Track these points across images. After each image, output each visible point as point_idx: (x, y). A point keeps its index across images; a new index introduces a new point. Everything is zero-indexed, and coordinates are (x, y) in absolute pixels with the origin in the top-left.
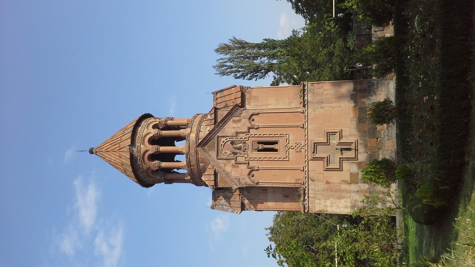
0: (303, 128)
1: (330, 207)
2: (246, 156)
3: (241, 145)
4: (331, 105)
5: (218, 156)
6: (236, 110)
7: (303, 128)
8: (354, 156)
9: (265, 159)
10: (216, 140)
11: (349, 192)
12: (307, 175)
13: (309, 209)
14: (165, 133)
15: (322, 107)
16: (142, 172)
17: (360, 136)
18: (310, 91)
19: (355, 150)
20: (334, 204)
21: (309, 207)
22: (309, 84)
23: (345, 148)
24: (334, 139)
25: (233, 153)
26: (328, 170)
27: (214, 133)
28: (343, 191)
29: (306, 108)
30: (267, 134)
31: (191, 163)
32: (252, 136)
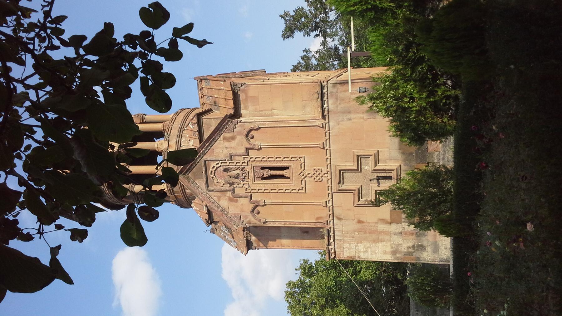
0: (324, 148)
1: (364, 252)
3: (238, 171)
4: (362, 115)
5: (208, 186)
6: (227, 124)
9: (273, 191)
10: (203, 165)
11: (389, 234)
12: (331, 212)
13: (335, 254)
15: (350, 119)
17: (405, 160)
18: (332, 96)
19: (397, 179)
21: (335, 252)
22: (329, 85)
24: (367, 164)
26: (359, 206)
28: (381, 232)
29: (327, 120)
30: (273, 157)
32: (252, 159)
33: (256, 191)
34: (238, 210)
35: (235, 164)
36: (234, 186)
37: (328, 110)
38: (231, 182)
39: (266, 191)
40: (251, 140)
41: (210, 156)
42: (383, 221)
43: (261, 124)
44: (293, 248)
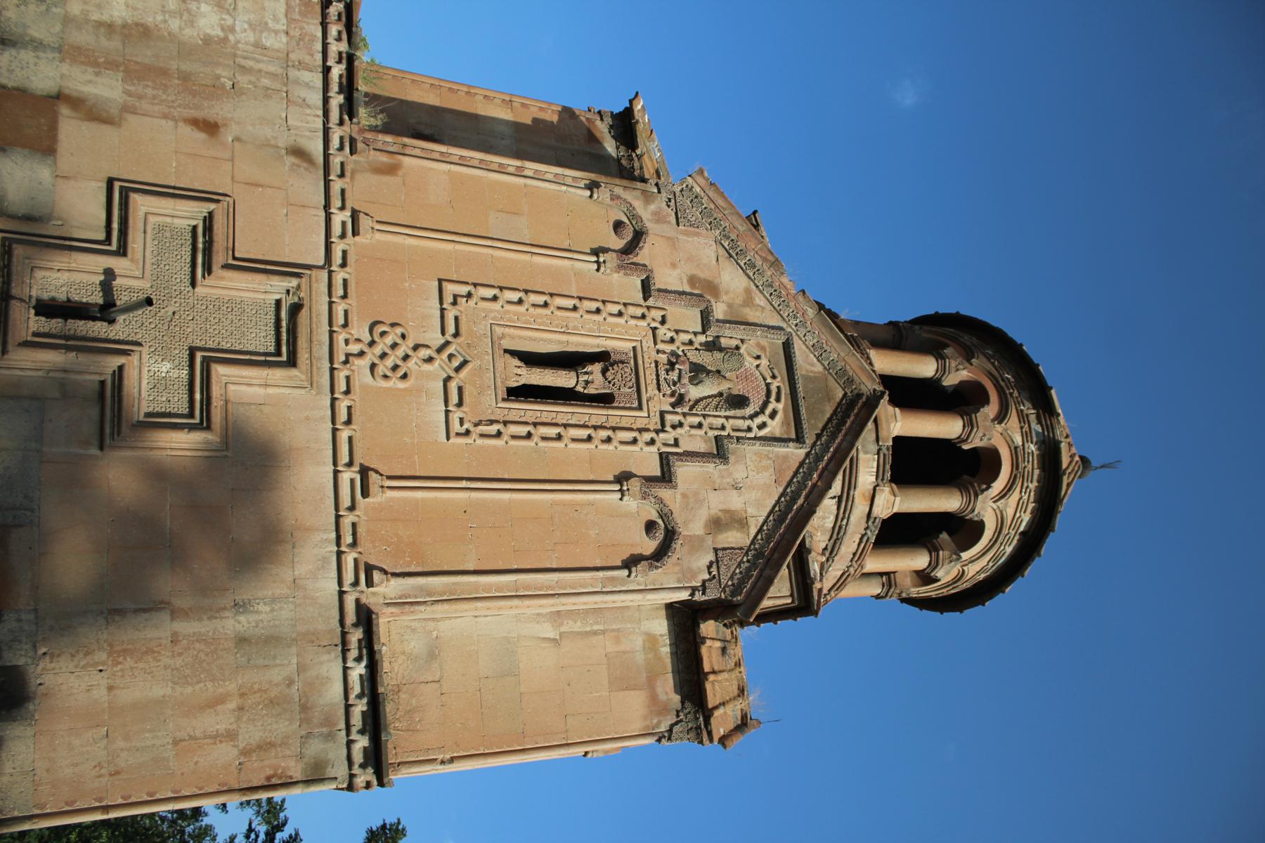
0: (364, 471)
3: (694, 392)
5: (787, 347)
6: (742, 582)
12: (336, 186)
14: (946, 502)
18: (328, 721)
21: (324, 26)
22: (341, 771)
24: (159, 384)
27: (819, 458)
28: (112, 65)
32: (647, 436)
36: (702, 339)
37: (345, 651)
38: (718, 355)
39: (593, 306)
40: (654, 516)
41: (785, 458)
43: (622, 582)
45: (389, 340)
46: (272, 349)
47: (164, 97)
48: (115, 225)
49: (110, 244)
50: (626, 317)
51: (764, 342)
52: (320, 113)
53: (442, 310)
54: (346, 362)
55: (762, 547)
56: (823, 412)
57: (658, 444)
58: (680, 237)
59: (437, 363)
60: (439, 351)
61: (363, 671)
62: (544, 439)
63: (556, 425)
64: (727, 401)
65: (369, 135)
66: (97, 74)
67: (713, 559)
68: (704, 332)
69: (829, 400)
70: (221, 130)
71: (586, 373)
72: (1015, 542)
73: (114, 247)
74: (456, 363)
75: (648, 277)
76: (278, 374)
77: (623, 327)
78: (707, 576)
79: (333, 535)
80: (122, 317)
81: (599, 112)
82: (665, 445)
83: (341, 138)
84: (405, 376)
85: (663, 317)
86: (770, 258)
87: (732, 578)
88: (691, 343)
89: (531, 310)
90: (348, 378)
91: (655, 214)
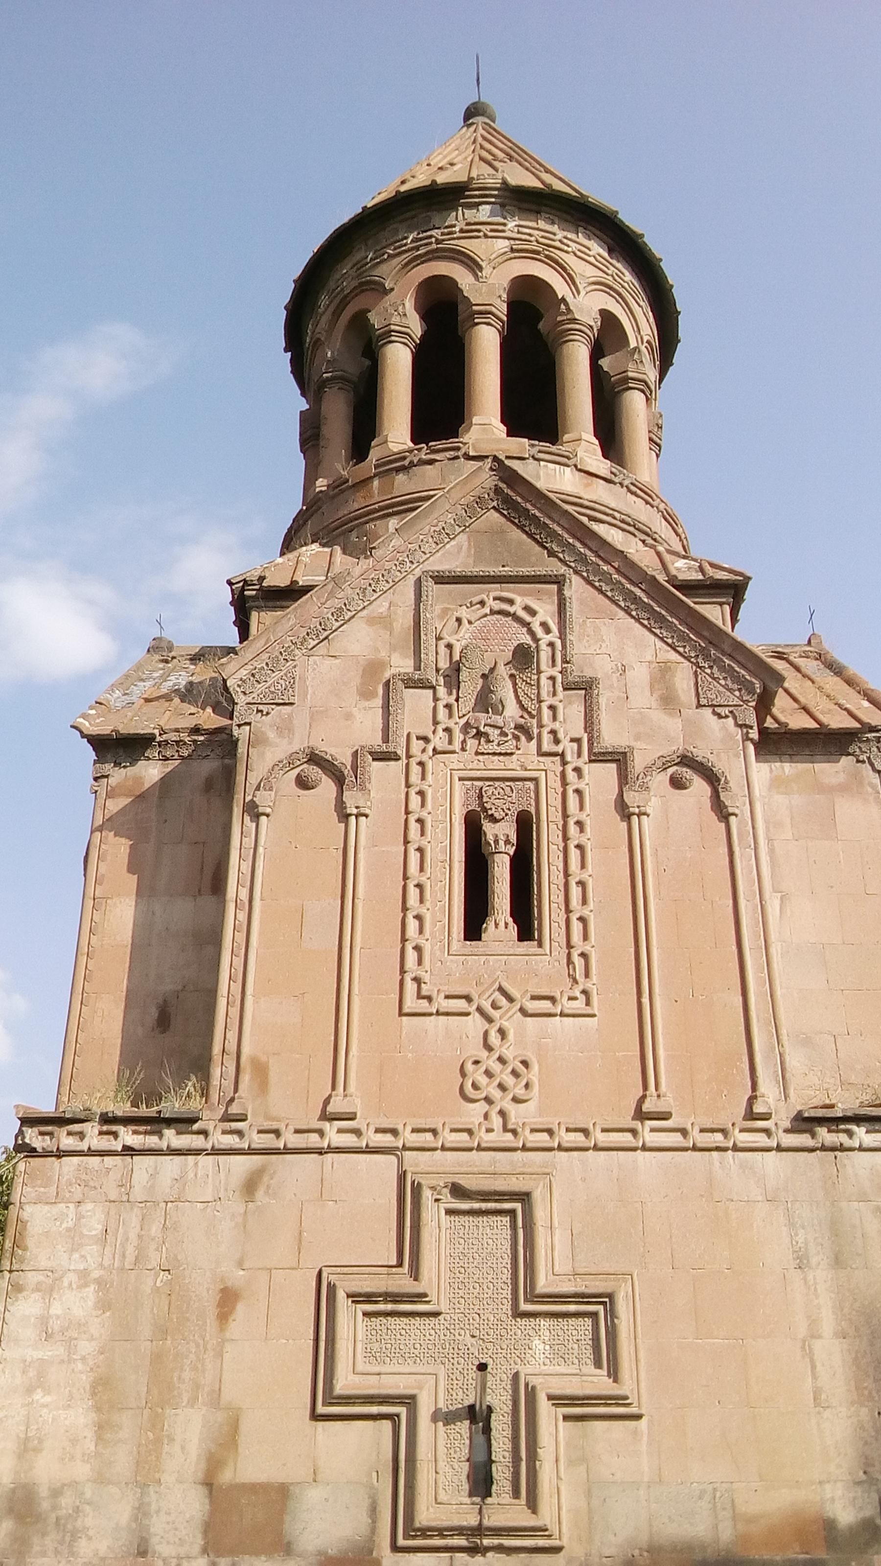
0: (641, 1115)
2: (439, 740)
5: (441, 579)
7: (641, 1115)
8: (425, 1515)
9: (414, 858)
11: (145, 1475)
16: (360, 265)
20: (60, 1351)
23: (496, 1442)
25: (456, 668)
26: (325, 1297)
27: (583, 559)
28: (156, 1422)
30: (584, 868)
31: (401, 477)
32: (571, 776)
33: (415, 778)
34: (321, 691)
35: (549, 700)
36: (442, 691)
37: (842, 1148)
38: (464, 675)
40: (663, 778)
41: (582, 602)
42: (227, 1439)
44: (84, 953)
45: (483, 1080)
46: (506, 1220)
47: (192, 1356)
48: (374, 1409)
49: (398, 1416)
50: (425, 787)
51: (438, 609)
52: (190, 1158)
53: (438, 1013)
54: (514, 1132)
55: (694, 648)
56: (520, 543)
57: (579, 763)
58: (308, 703)
59: (506, 1024)
60: (490, 1020)
61: (863, 1130)
62: (584, 901)
63: (566, 885)
64: (522, 670)
65: (214, 1097)
66: (171, 1440)
67: (710, 710)
68: (433, 688)
69: (503, 532)
70: (229, 1284)
71: (496, 842)
72: (619, 265)
73: (402, 1411)
74: (503, 1001)
75: (371, 753)
76: (540, 1214)
77: (436, 792)
78: (730, 720)
79: (715, 1154)
80: (488, 1398)
81: (96, 779)
82: (579, 755)
83: (224, 1132)
84: (525, 1063)
85: (418, 738)
86: (330, 586)
87: (730, 690)
88: (448, 706)
89: (428, 904)
90: (533, 1131)
91: (279, 730)
